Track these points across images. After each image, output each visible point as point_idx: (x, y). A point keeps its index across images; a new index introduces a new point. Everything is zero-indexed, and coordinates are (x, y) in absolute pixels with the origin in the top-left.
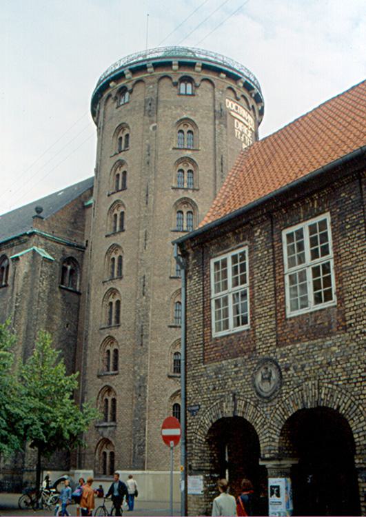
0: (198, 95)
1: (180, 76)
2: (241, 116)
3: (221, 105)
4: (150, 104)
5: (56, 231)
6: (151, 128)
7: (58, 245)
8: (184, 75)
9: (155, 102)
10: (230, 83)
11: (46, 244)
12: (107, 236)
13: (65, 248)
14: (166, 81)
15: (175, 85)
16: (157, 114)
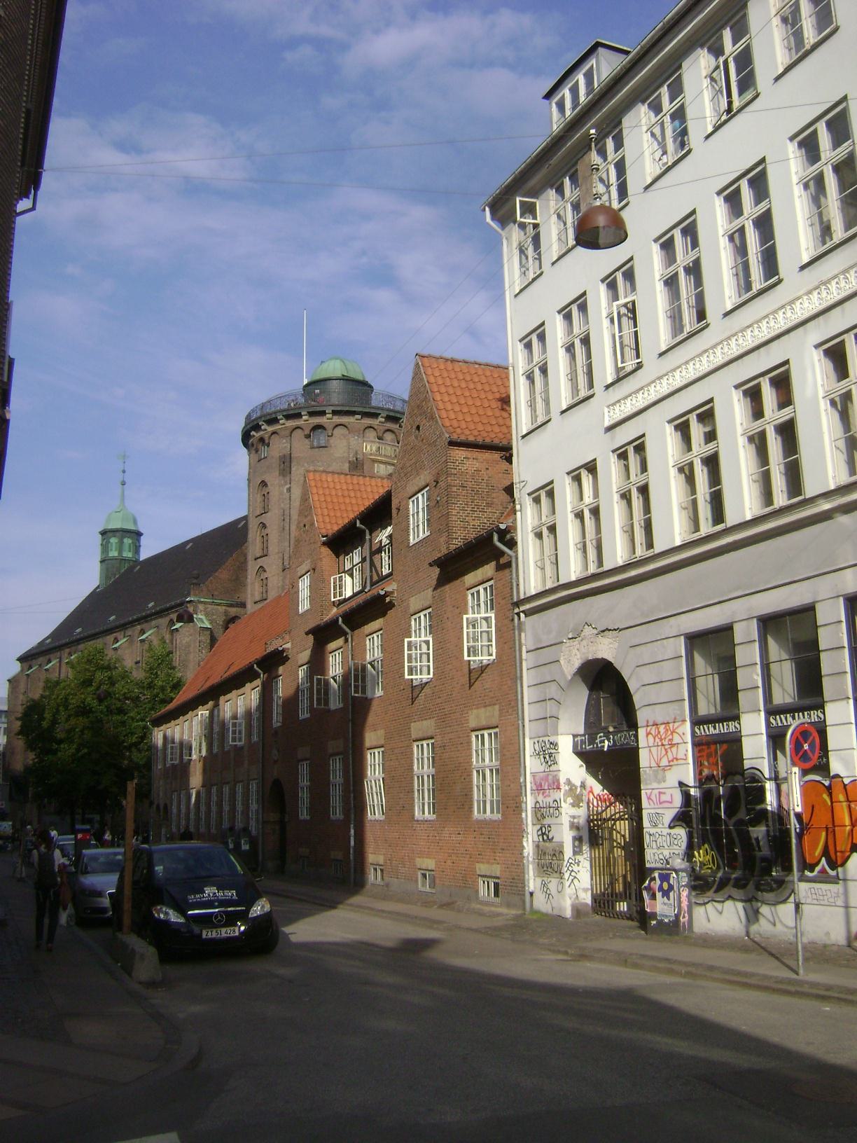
0: (331, 446)
1: (312, 426)
2: (385, 456)
3: (356, 453)
4: (284, 463)
5: (216, 593)
6: (285, 491)
7: (219, 607)
8: (315, 424)
9: (288, 460)
10: (368, 421)
11: (206, 609)
12: (255, 603)
13: (227, 608)
14: (299, 431)
15: (308, 436)
16: (290, 473)
